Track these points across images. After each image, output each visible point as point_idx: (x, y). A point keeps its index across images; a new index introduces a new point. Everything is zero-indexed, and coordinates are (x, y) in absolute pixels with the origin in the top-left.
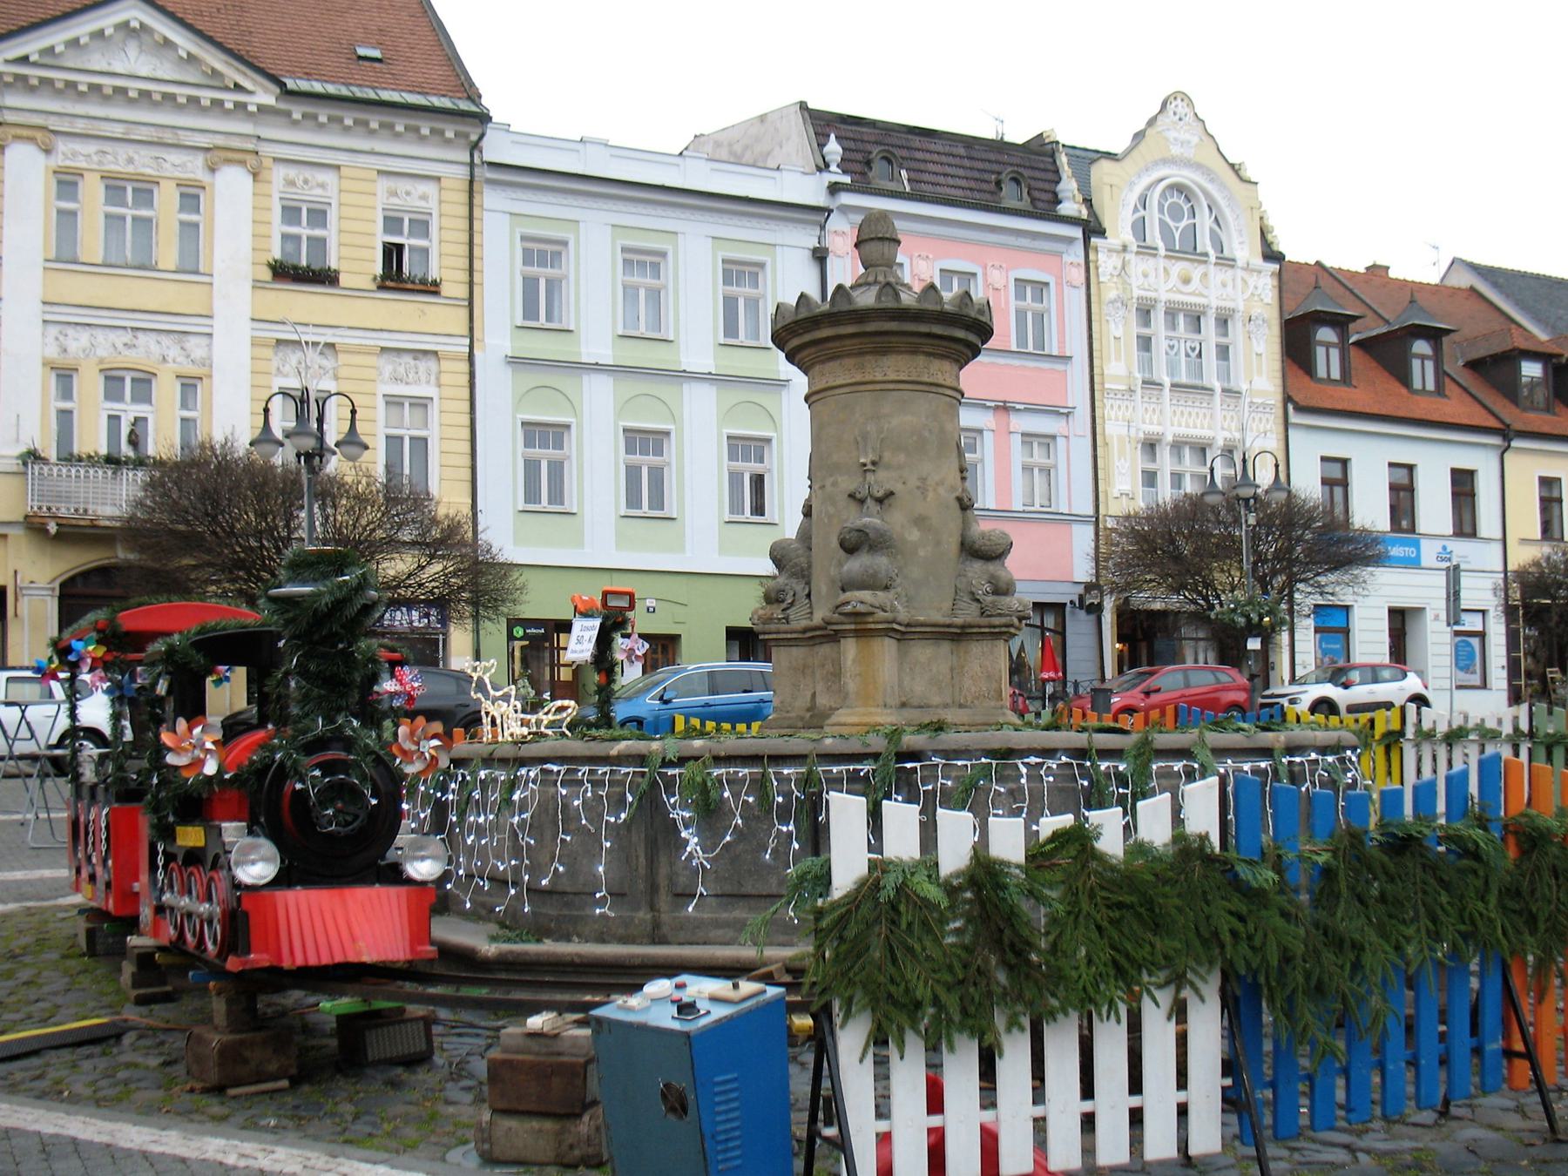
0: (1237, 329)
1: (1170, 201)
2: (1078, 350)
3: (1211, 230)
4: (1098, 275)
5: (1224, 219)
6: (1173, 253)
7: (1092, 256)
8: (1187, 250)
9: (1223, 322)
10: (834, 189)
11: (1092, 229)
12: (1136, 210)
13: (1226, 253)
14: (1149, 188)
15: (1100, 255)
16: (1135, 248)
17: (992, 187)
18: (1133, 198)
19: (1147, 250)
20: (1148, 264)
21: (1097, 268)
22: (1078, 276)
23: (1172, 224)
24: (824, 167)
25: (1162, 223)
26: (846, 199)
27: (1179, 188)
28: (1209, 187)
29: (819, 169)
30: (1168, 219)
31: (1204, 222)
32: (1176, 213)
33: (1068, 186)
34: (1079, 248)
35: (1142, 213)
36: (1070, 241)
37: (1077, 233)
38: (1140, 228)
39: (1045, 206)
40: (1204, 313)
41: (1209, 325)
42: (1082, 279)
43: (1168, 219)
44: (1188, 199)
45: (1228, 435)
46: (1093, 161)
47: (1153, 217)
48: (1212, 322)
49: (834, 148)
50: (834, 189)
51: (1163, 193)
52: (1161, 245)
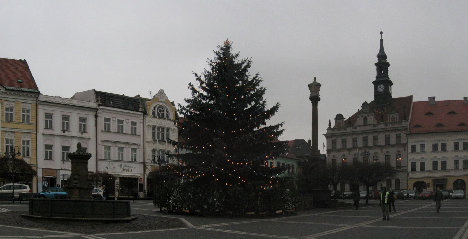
0: (171, 132)
1: (159, 108)
2: (142, 134)
3: (166, 114)
4: (146, 121)
5: (169, 112)
6: (159, 118)
7: (145, 118)
8: (162, 117)
9: (168, 130)
10: (99, 105)
11: (145, 113)
12: (153, 110)
13: (169, 118)
14: (156, 106)
15: (146, 118)
16: (152, 117)
17: (127, 105)
18: (152, 108)
19: (155, 117)
20: (154, 120)
21: (145, 120)
22: (142, 121)
23: (160, 113)
24: (97, 101)
25: (158, 112)
26: (101, 107)
27: (161, 106)
28: (166, 106)
29: (96, 102)
30: (159, 112)
31: (165, 113)
32: (160, 111)
33: (141, 106)
34: (142, 116)
35: (154, 110)
36: (141, 115)
37: (142, 114)
38: (153, 113)
39: (136, 109)
40: (165, 128)
41: (165, 130)
42: (143, 122)
43: (159, 112)
44: (162, 109)
45: (168, 149)
46: (146, 101)
47: (156, 111)
48: (166, 130)
49: (99, 99)
50: (99, 105)
51: (158, 108)
52: (157, 116)
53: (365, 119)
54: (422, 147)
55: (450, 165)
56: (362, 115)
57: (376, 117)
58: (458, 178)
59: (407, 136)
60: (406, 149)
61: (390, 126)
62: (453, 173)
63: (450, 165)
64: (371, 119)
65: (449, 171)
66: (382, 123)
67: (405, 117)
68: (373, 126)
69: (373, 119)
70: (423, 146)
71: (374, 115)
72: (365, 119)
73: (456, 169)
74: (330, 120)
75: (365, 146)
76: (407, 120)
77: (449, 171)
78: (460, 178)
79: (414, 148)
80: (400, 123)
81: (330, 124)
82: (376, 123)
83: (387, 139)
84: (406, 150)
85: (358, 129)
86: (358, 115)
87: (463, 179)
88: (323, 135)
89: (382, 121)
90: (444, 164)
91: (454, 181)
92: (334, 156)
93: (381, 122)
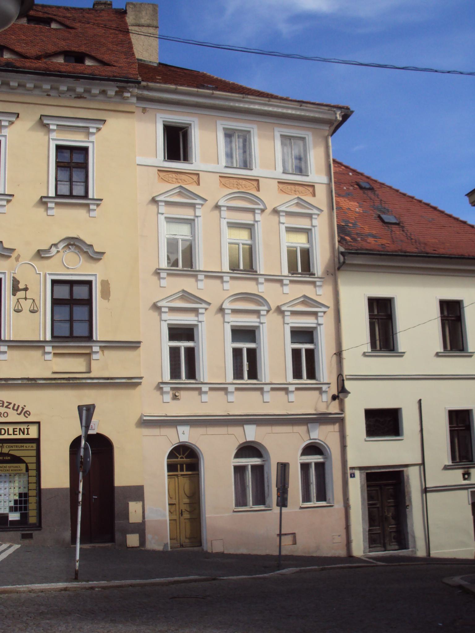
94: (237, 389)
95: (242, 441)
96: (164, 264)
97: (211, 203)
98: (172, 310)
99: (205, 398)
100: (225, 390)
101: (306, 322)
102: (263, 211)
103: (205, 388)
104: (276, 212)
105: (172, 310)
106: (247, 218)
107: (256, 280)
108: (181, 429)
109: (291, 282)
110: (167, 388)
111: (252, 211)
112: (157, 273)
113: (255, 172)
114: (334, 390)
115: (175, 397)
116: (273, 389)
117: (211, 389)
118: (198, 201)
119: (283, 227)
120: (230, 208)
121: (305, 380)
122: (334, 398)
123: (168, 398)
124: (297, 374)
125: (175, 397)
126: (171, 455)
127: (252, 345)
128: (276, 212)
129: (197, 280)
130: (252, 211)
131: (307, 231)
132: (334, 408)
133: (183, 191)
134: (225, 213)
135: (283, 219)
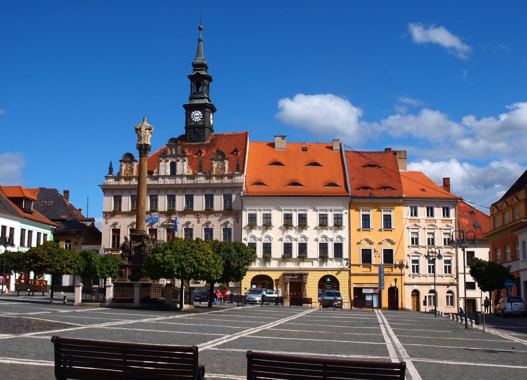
53: (173, 166)
54: (267, 218)
55: (313, 251)
56: (168, 159)
57: (189, 164)
58: (326, 273)
59: (241, 199)
60: (240, 219)
61: (214, 181)
62: (316, 265)
63: (313, 251)
64: (183, 167)
65: (312, 260)
66: (200, 176)
67: (239, 168)
68: (185, 179)
69: (185, 167)
70: (268, 216)
71: (187, 160)
72: (173, 166)
73: (323, 258)
74: (111, 163)
75: (171, 212)
76: (243, 172)
77: (312, 260)
78: (330, 273)
79: (252, 218)
80: (230, 177)
81: (111, 170)
82: (191, 173)
83: (209, 200)
84: (240, 222)
85: (161, 181)
86: (161, 159)
87: (334, 275)
88: (99, 186)
89: (200, 171)
90: (303, 248)
91: (321, 277)
92: (115, 224)
93: (199, 174)
94: (429, 276)
95: (430, 289)
96: (410, 244)
97: (423, 228)
98: (413, 256)
99: (421, 278)
100: (426, 276)
101: (449, 258)
102: (437, 229)
103: (421, 276)
104: (440, 229)
105: (413, 256)
106: (432, 231)
107: (419, 247)
108: (415, 286)
109: (444, 248)
110: (411, 276)
111: (434, 229)
112: (409, 247)
113: (435, 218)
114: (455, 277)
115: (413, 278)
116: (439, 276)
117: (422, 276)
118: (419, 227)
119: (442, 233)
120: (428, 229)
121: (448, 274)
122: (456, 279)
123: (411, 278)
124: (446, 272)
125: (413, 278)
126: (413, 292)
127: (417, 264)
128: (440, 229)
129: (419, 248)
130: (434, 229)
131: (449, 234)
132: (455, 282)
133: (415, 225)
134: (426, 230)
135: (442, 231)
